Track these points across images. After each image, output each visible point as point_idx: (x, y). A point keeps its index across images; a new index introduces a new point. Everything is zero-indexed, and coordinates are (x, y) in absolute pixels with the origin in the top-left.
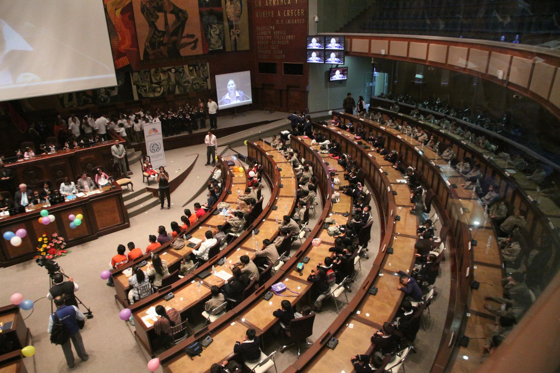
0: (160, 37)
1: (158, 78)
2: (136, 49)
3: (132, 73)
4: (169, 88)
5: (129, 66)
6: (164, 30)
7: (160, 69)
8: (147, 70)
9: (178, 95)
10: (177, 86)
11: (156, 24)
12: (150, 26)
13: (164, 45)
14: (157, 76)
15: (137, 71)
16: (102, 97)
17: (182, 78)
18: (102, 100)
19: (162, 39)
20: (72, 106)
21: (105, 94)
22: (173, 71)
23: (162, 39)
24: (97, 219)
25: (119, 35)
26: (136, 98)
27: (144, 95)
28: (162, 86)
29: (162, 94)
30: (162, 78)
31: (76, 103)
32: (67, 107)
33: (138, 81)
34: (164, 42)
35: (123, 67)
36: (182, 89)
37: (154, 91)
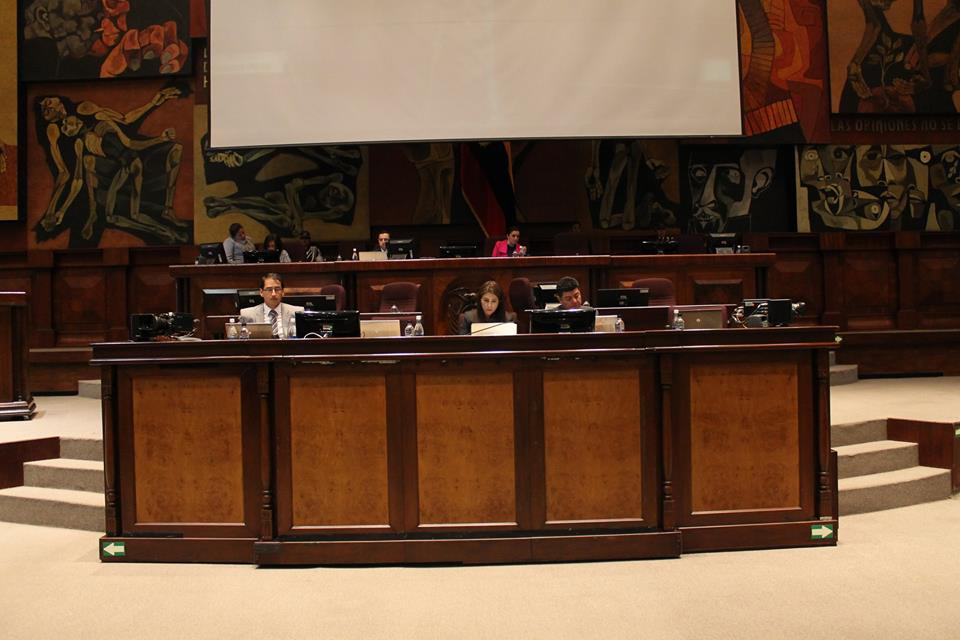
0: (897, 52)
1: (877, 174)
2: (819, 83)
3: (802, 147)
4: (907, 208)
5: (795, 127)
6: (910, 33)
7: (884, 148)
8: (848, 147)
9: (934, 235)
10: (933, 207)
11: (886, 14)
12: (868, 20)
13: (907, 76)
14: (875, 168)
15: (816, 147)
16: (704, 215)
17: (952, 181)
18: (704, 224)
19: (900, 58)
20: (619, 227)
21: (713, 209)
22: (925, 157)
23: (900, 58)
24: (697, 452)
25: (777, 40)
26: (803, 225)
27: (828, 219)
28: (885, 199)
29: (882, 225)
30: (889, 177)
31: (632, 219)
32: (605, 225)
33: (815, 177)
34: (908, 67)
35: (777, 129)
36: (948, 214)
37: (860, 211)
